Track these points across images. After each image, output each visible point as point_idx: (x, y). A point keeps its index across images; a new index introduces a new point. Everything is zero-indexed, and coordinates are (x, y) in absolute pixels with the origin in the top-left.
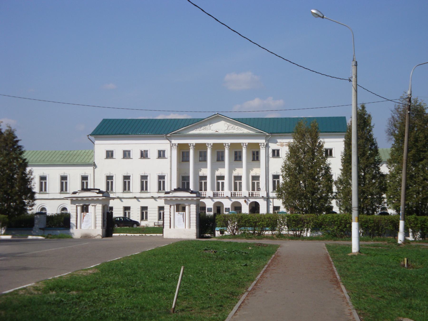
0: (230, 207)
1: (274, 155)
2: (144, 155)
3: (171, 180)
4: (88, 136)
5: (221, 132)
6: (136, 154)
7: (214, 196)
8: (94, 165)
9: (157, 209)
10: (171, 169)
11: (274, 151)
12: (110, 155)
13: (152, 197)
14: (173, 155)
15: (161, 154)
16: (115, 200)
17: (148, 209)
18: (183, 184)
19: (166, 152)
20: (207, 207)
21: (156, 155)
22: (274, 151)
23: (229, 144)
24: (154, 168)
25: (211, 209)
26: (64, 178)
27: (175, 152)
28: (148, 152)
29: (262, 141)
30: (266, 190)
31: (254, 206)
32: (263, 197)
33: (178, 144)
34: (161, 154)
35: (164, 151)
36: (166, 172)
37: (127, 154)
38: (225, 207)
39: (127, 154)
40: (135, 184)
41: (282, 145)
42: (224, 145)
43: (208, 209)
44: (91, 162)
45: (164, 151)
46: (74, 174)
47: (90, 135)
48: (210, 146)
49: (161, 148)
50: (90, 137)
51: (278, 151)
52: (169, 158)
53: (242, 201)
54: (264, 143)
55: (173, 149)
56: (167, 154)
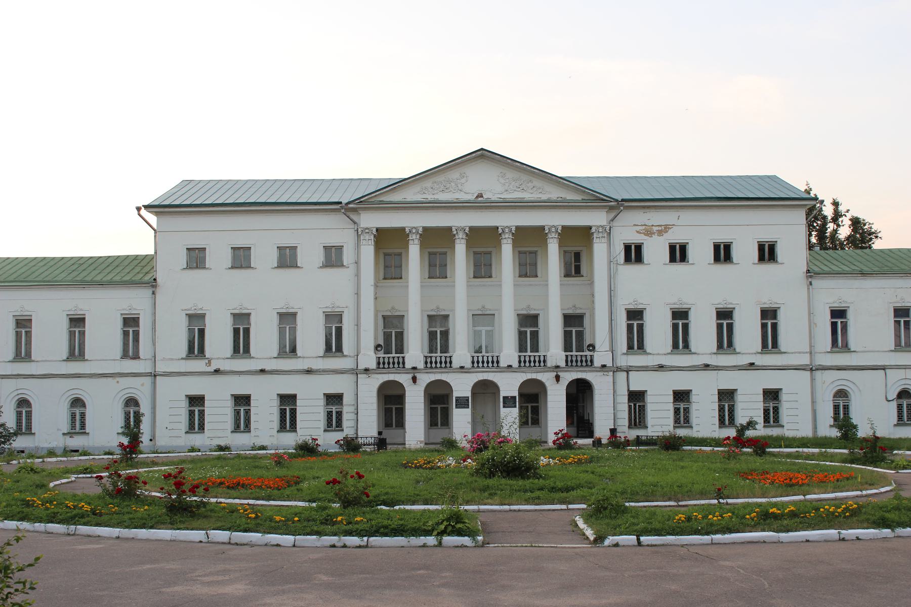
1: (628, 259)
2: (287, 258)
3: (358, 325)
4: (139, 209)
6: (264, 256)
7: (567, 365)
9: (322, 402)
10: (358, 294)
15: (333, 257)
17: (299, 403)
18: (387, 336)
19: (345, 249)
20: (456, 394)
21: (320, 257)
22: (627, 248)
23: (514, 229)
24: (314, 292)
25: (467, 399)
26: (77, 322)
27: (368, 250)
28: (298, 250)
31: (574, 391)
32: (604, 366)
33: (377, 230)
34: (333, 257)
35: (340, 249)
36: (343, 301)
38: (503, 394)
39: (241, 258)
40: (265, 338)
41: (649, 233)
42: (500, 231)
43: (458, 399)
44: (147, 278)
45: (340, 249)
46: (104, 310)
47: (146, 207)
48: (461, 235)
49: (334, 241)
50: (143, 212)
51: (639, 248)
52: (352, 268)
53: (546, 378)
55: (363, 242)
56: (348, 257)
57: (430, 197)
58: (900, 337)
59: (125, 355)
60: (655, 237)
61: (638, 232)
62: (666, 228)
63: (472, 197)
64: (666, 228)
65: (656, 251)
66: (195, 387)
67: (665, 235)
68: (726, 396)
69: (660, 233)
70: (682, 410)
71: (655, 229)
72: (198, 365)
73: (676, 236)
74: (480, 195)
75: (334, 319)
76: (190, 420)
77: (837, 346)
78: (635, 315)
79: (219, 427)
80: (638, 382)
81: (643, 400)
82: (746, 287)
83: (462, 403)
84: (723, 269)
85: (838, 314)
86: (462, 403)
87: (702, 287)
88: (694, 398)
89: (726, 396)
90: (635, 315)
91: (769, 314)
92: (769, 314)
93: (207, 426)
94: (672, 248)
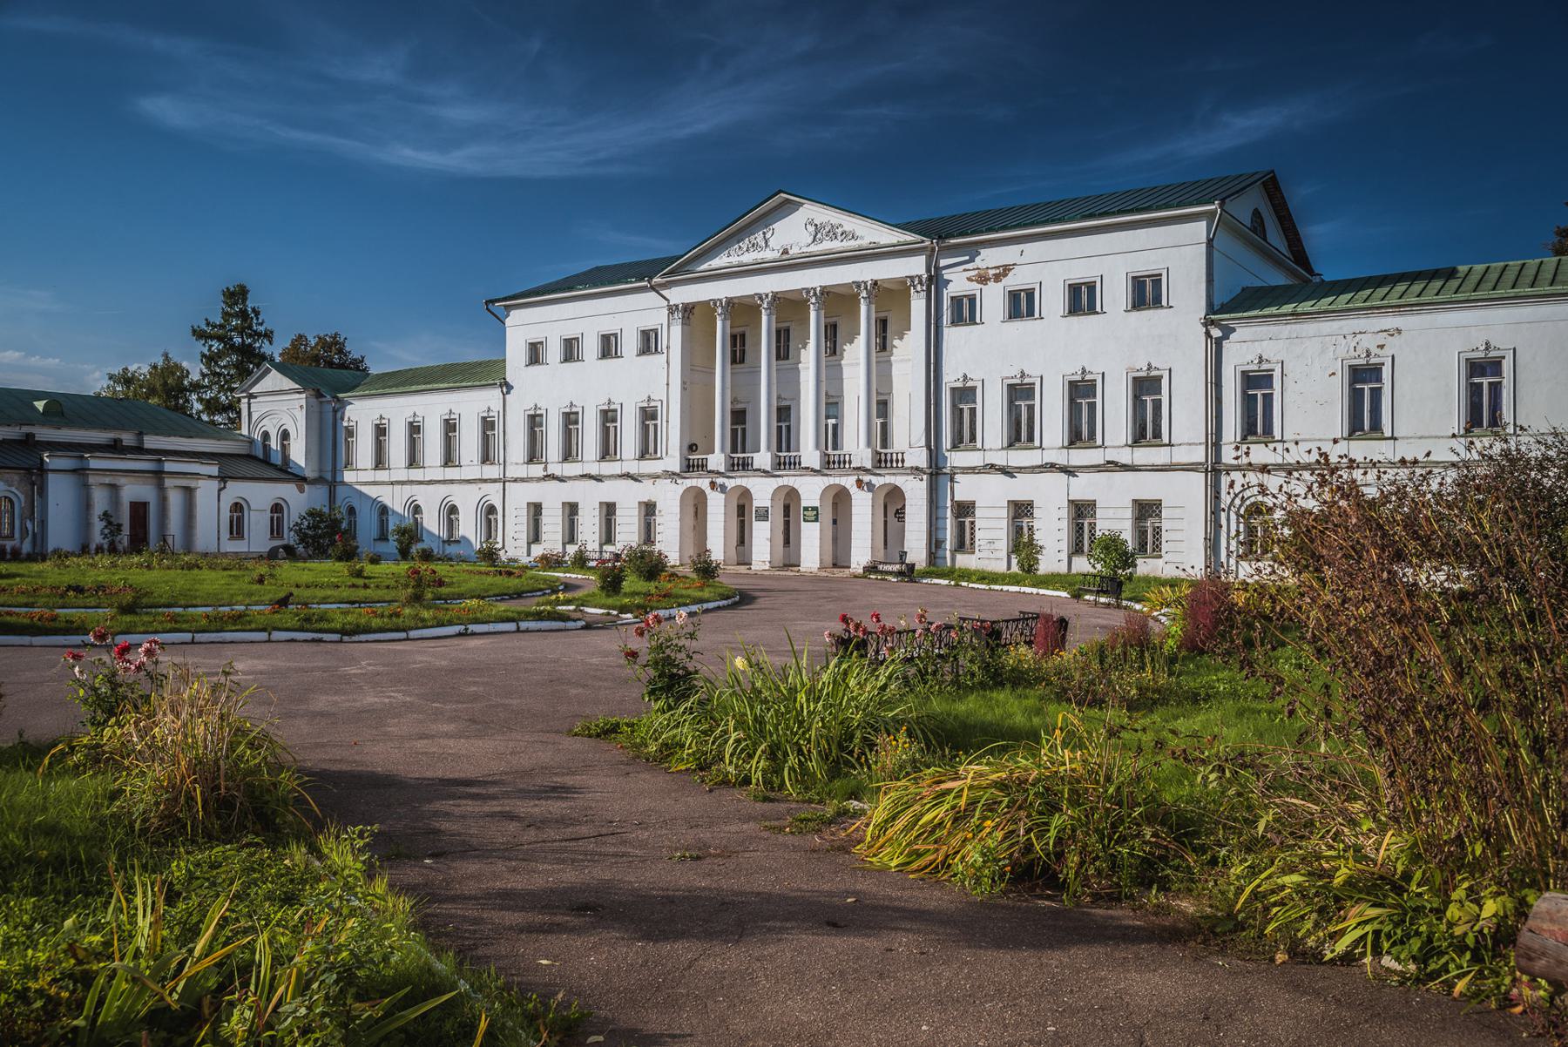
0: (768, 504)
5: (794, 251)
8: (507, 387)
11: (957, 301)
12: (535, 354)
13: (628, 476)
14: (674, 337)
15: (649, 342)
16: (607, 483)
20: (756, 504)
29: (916, 266)
30: (928, 446)
37: (571, 351)
41: (983, 279)
49: (649, 324)
54: (920, 277)
57: (734, 260)
58: (961, 423)
59: (446, 465)
60: (991, 284)
61: (969, 279)
62: (1006, 270)
63: (776, 255)
64: (1006, 270)
65: (993, 300)
66: (534, 492)
67: (1005, 281)
68: (1081, 511)
69: (997, 278)
70: (1025, 529)
71: (991, 272)
72: (537, 470)
73: (1015, 281)
74: (785, 252)
75: (648, 415)
76: (835, 540)
77: (1255, 433)
78: (964, 394)
79: (552, 539)
80: (964, 489)
81: (1159, 516)
82: (1113, 346)
83: (814, 514)
84: (1083, 324)
85: (1256, 382)
86: (763, 515)
87: (1052, 350)
88: (1036, 513)
89: (1081, 511)
90: (964, 394)
91: (1145, 387)
92: (1145, 387)
93: (544, 537)
94: (1014, 296)
